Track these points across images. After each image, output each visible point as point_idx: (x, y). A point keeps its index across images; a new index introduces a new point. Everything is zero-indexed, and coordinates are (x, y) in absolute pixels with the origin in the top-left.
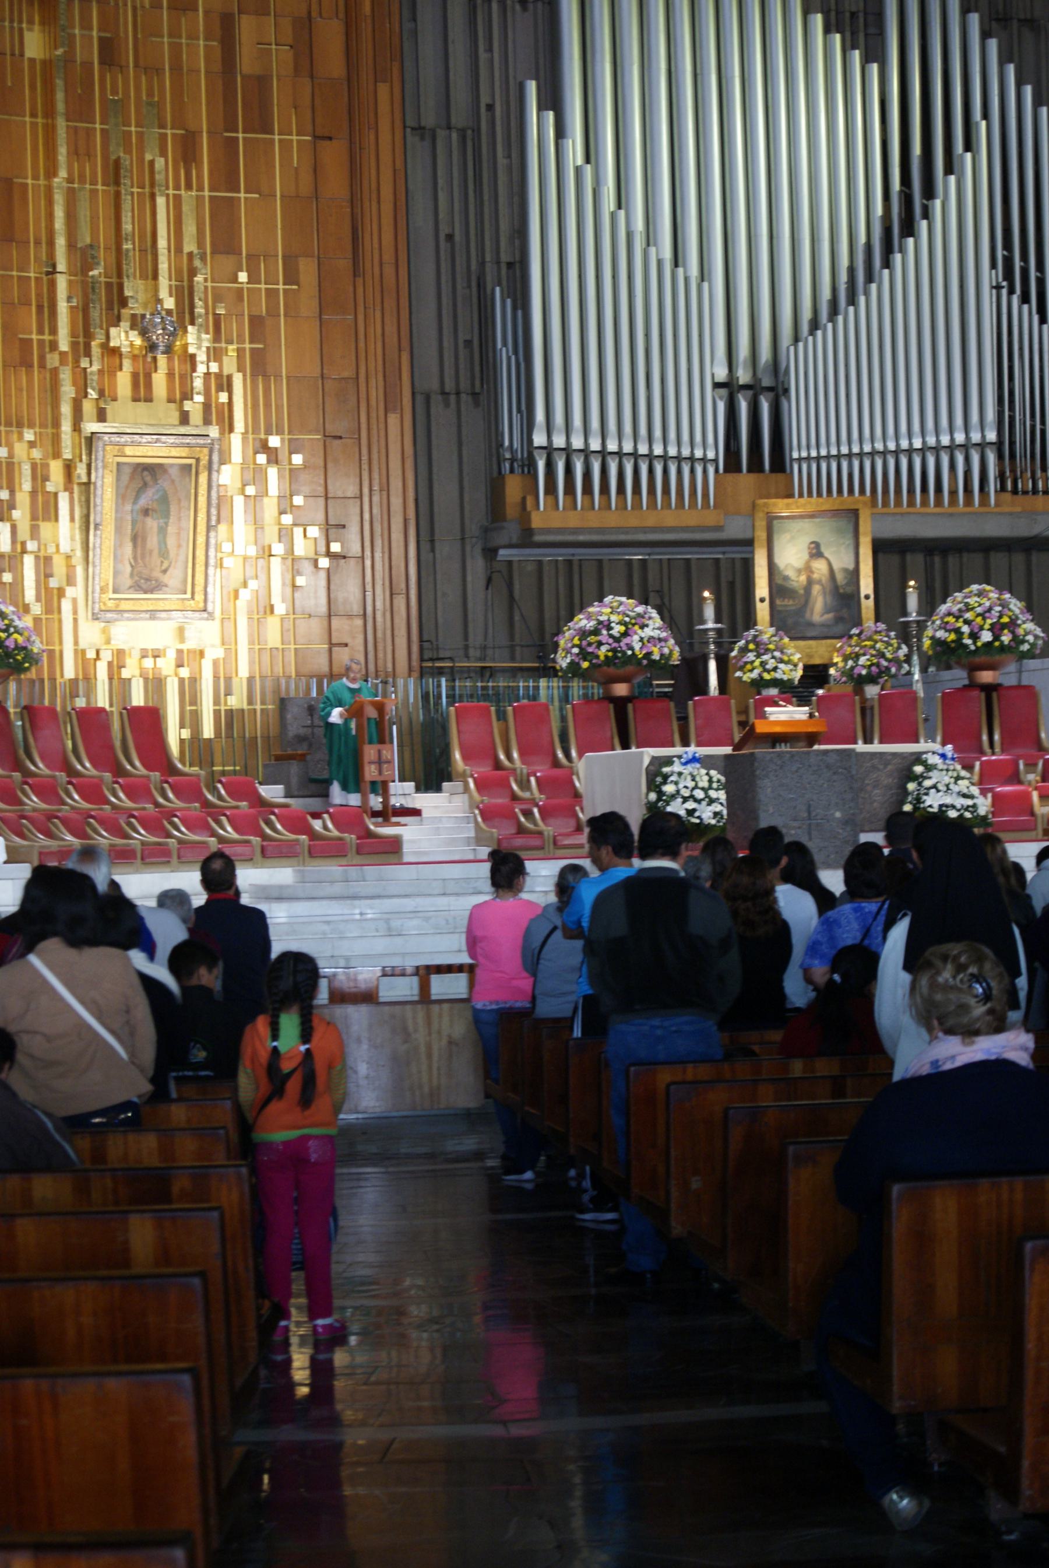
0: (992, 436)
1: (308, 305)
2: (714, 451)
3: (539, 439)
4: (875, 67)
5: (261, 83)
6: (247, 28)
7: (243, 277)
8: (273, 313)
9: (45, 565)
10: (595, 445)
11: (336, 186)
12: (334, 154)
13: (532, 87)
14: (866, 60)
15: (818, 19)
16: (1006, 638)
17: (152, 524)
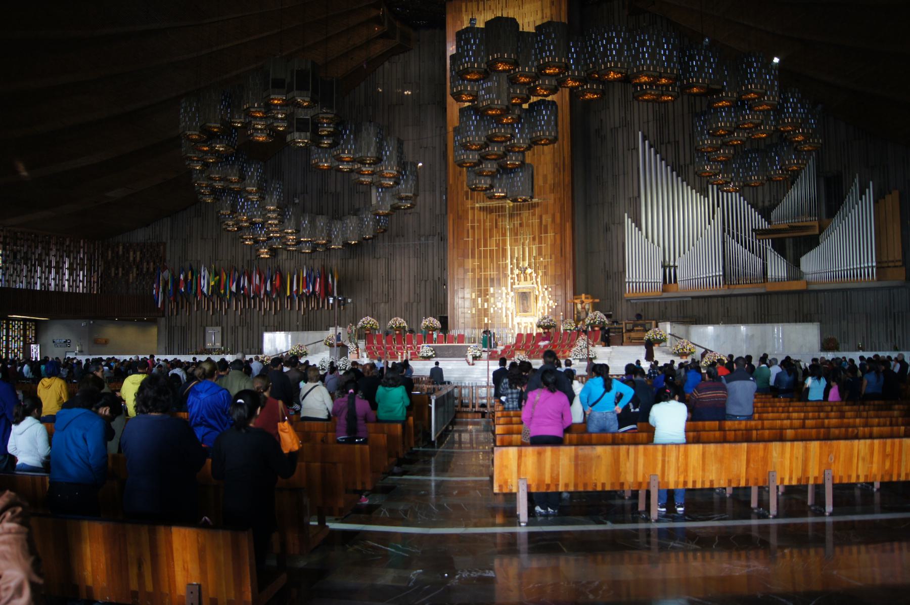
0: (721, 273)
1: (553, 263)
2: (661, 280)
3: (627, 280)
4: (706, 199)
5: (546, 226)
6: (544, 217)
7: (542, 259)
8: (548, 264)
9: (507, 309)
10: (653, 281)
11: (558, 241)
12: (558, 237)
13: (626, 215)
14: (704, 198)
15: (694, 191)
16: (592, 322)
17: (525, 302)
